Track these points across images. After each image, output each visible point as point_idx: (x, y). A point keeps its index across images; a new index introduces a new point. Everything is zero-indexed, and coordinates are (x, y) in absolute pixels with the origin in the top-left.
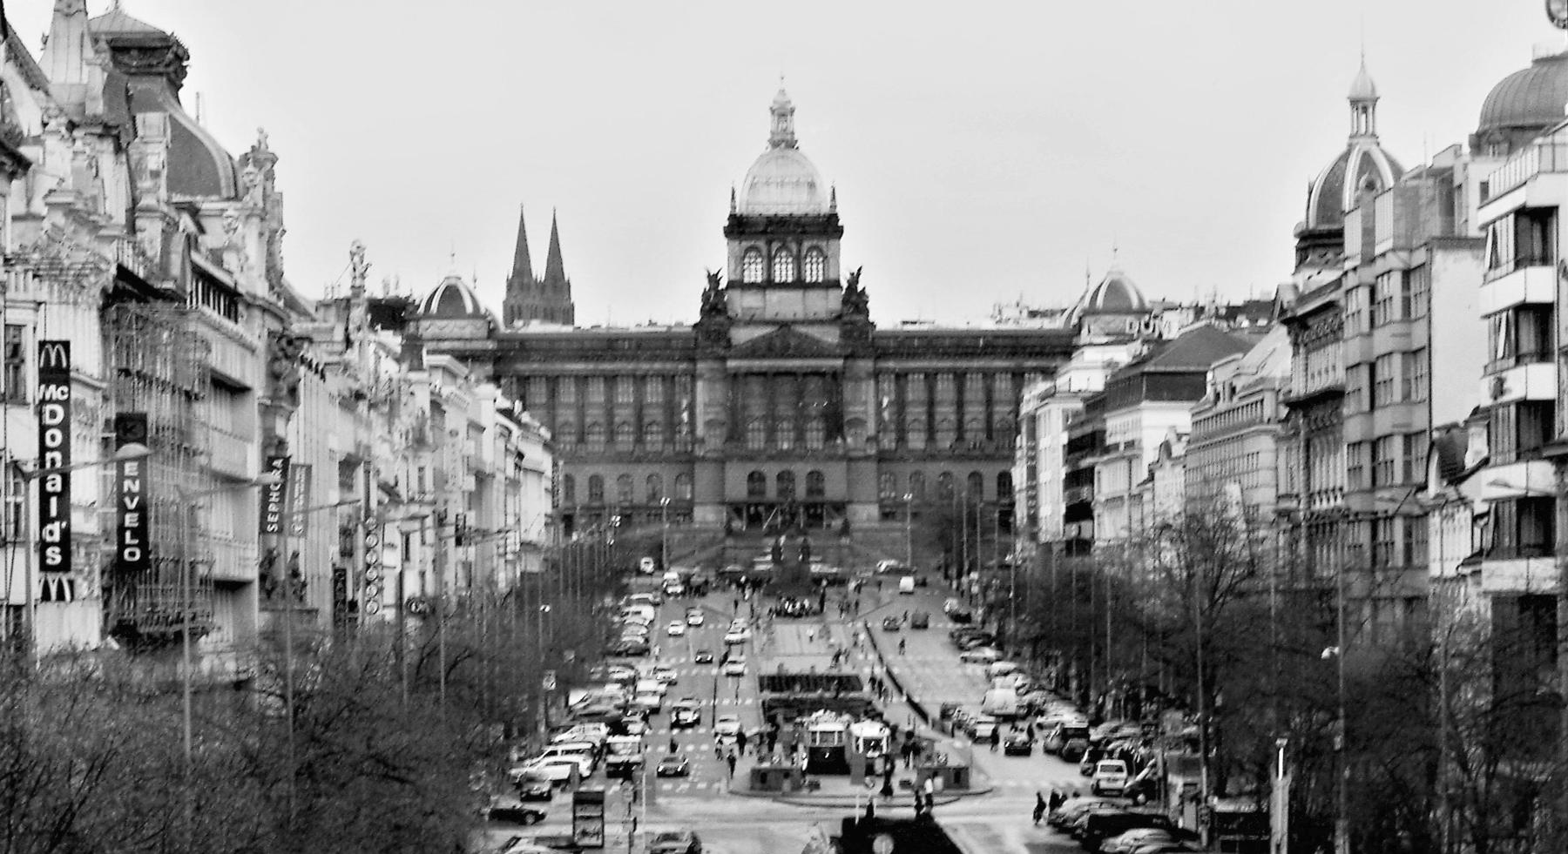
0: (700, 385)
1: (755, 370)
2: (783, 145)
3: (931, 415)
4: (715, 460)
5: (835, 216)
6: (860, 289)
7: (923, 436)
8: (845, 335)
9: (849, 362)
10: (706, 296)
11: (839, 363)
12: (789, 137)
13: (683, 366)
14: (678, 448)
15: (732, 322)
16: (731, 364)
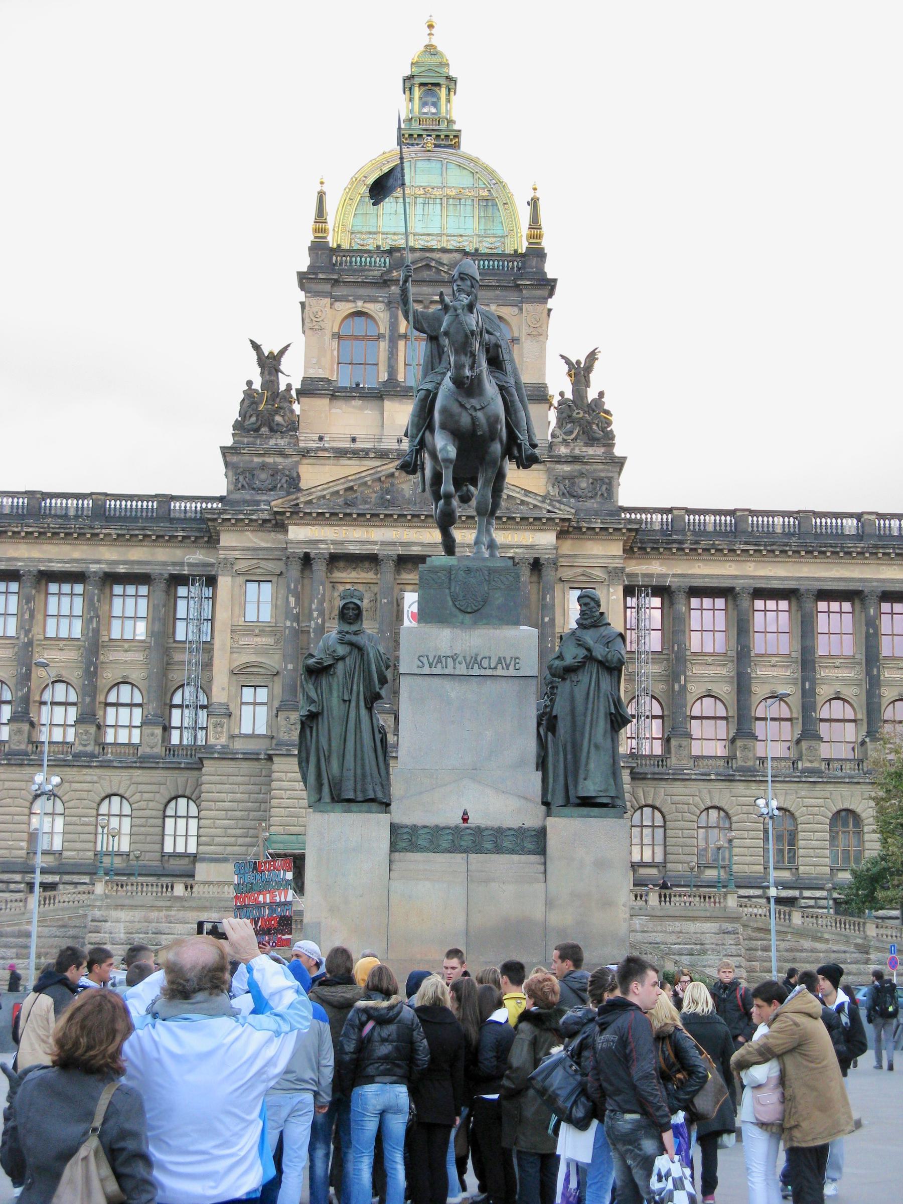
0: (224, 582)
1: (353, 549)
2: (430, 142)
3: (743, 685)
4: (251, 757)
5: (537, 254)
6: (592, 394)
7: (722, 730)
8: (557, 480)
9: (567, 547)
10: (250, 399)
11: (546, 539)
12: (443, 126)
13: (197, 556)
14: (175, 738)
15: (305, 454)
16: (298, 533)
